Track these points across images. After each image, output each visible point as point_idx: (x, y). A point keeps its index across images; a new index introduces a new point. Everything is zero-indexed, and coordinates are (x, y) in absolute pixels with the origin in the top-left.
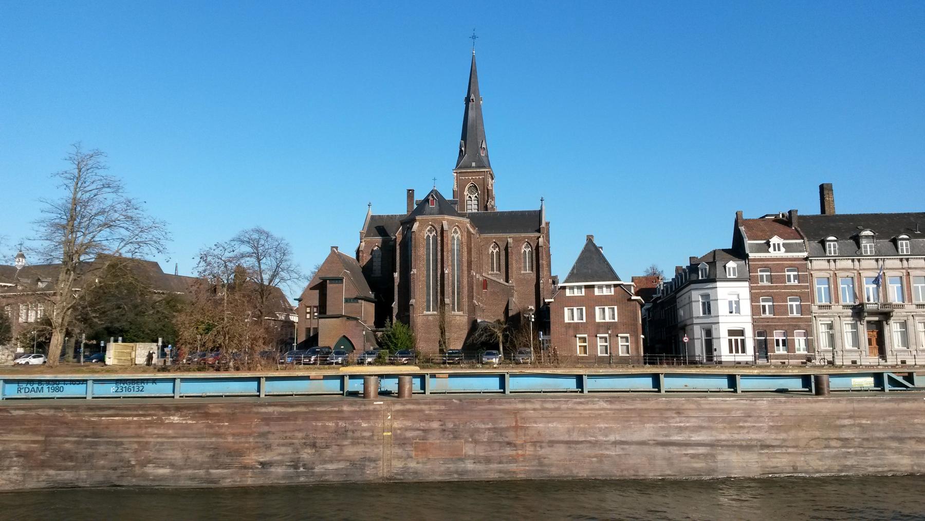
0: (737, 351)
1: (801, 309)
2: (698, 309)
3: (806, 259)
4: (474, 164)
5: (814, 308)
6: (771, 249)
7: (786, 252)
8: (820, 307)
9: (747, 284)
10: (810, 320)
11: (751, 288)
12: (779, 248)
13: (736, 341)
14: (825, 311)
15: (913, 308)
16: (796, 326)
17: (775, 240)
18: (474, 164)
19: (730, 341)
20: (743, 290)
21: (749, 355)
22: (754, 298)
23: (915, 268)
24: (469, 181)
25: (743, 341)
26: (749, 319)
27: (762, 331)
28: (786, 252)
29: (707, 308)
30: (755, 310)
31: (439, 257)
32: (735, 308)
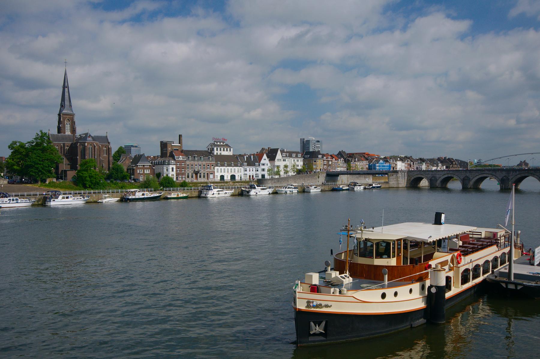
2: (165, 170)
12: (181, 158)
20: (174, 167)
22: (176, 168)
27: (177, 174)
29: (167, 170)
30: (177, 171)
32: (173, 170)
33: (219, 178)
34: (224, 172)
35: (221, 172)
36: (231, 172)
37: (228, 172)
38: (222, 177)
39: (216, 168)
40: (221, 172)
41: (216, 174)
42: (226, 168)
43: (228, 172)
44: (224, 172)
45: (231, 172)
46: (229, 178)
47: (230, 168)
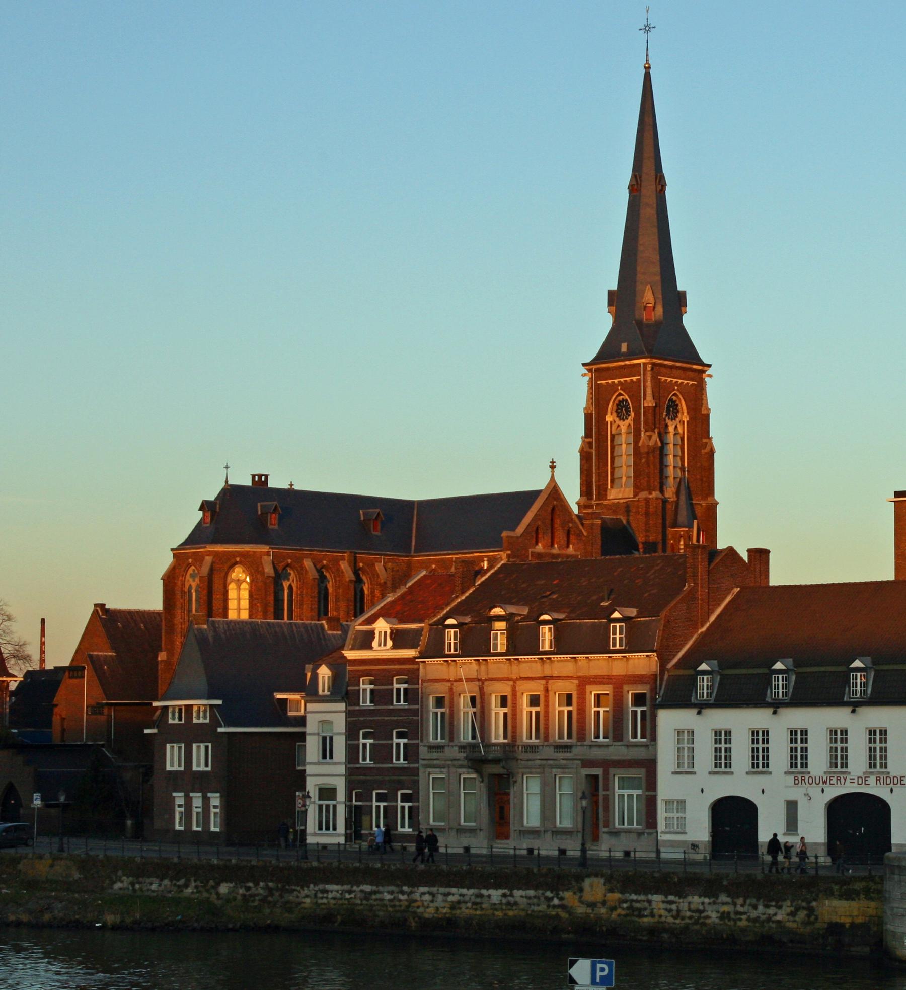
0: (328, 829)
1: (411, 753)
3: (411, 661)
4: (624, 348)
5: (423, 751)
6: (375, 644)
7: (395, 647)
8: (432, 748)
9: (342, 706)
10: (415, 772)
11: (349, 713)
13: (328, 806)
14: (435, 755)
15: (549, 752)
16: (399, 782)
17: (382, 626)
18: (624, 348)
19: (320, 807)
21: (337, 837)
22: (351, 733)
23: (558, 678)
24: (613, 388)
25: (335, 806)
26: (342, 770)
28: (395, 647)
30: (352, 752)
31: (358, 605)
32: (327, 751)
33: (699, 829)
34: (760, 761)
35: (723, 761)
36: (839, 759)
37: (798, 759)
38: (734, 816)
39: (670, 721)
40: (723, 761)
41: (668, 786)
42: (780, 724)
43: (798, 759)
44: (760, 761)
45: (839, 759)
46: (814, 830)
47: (818, 721)
